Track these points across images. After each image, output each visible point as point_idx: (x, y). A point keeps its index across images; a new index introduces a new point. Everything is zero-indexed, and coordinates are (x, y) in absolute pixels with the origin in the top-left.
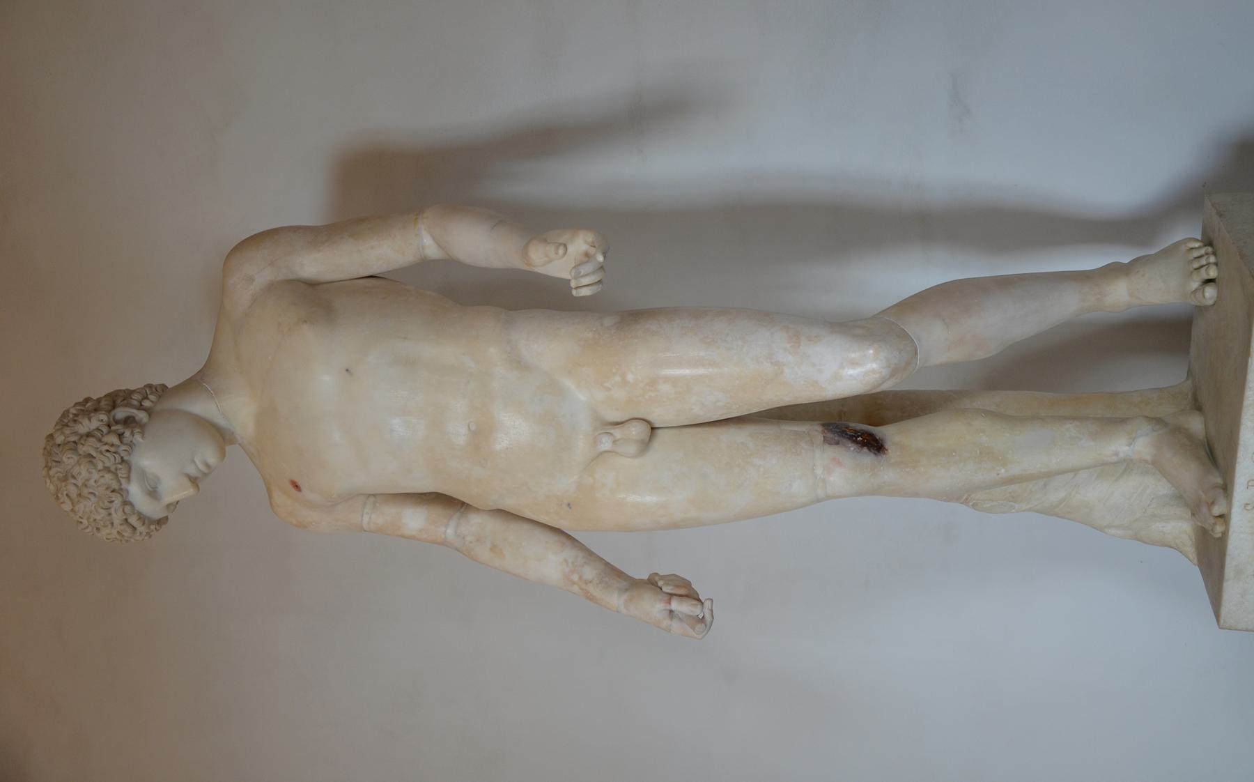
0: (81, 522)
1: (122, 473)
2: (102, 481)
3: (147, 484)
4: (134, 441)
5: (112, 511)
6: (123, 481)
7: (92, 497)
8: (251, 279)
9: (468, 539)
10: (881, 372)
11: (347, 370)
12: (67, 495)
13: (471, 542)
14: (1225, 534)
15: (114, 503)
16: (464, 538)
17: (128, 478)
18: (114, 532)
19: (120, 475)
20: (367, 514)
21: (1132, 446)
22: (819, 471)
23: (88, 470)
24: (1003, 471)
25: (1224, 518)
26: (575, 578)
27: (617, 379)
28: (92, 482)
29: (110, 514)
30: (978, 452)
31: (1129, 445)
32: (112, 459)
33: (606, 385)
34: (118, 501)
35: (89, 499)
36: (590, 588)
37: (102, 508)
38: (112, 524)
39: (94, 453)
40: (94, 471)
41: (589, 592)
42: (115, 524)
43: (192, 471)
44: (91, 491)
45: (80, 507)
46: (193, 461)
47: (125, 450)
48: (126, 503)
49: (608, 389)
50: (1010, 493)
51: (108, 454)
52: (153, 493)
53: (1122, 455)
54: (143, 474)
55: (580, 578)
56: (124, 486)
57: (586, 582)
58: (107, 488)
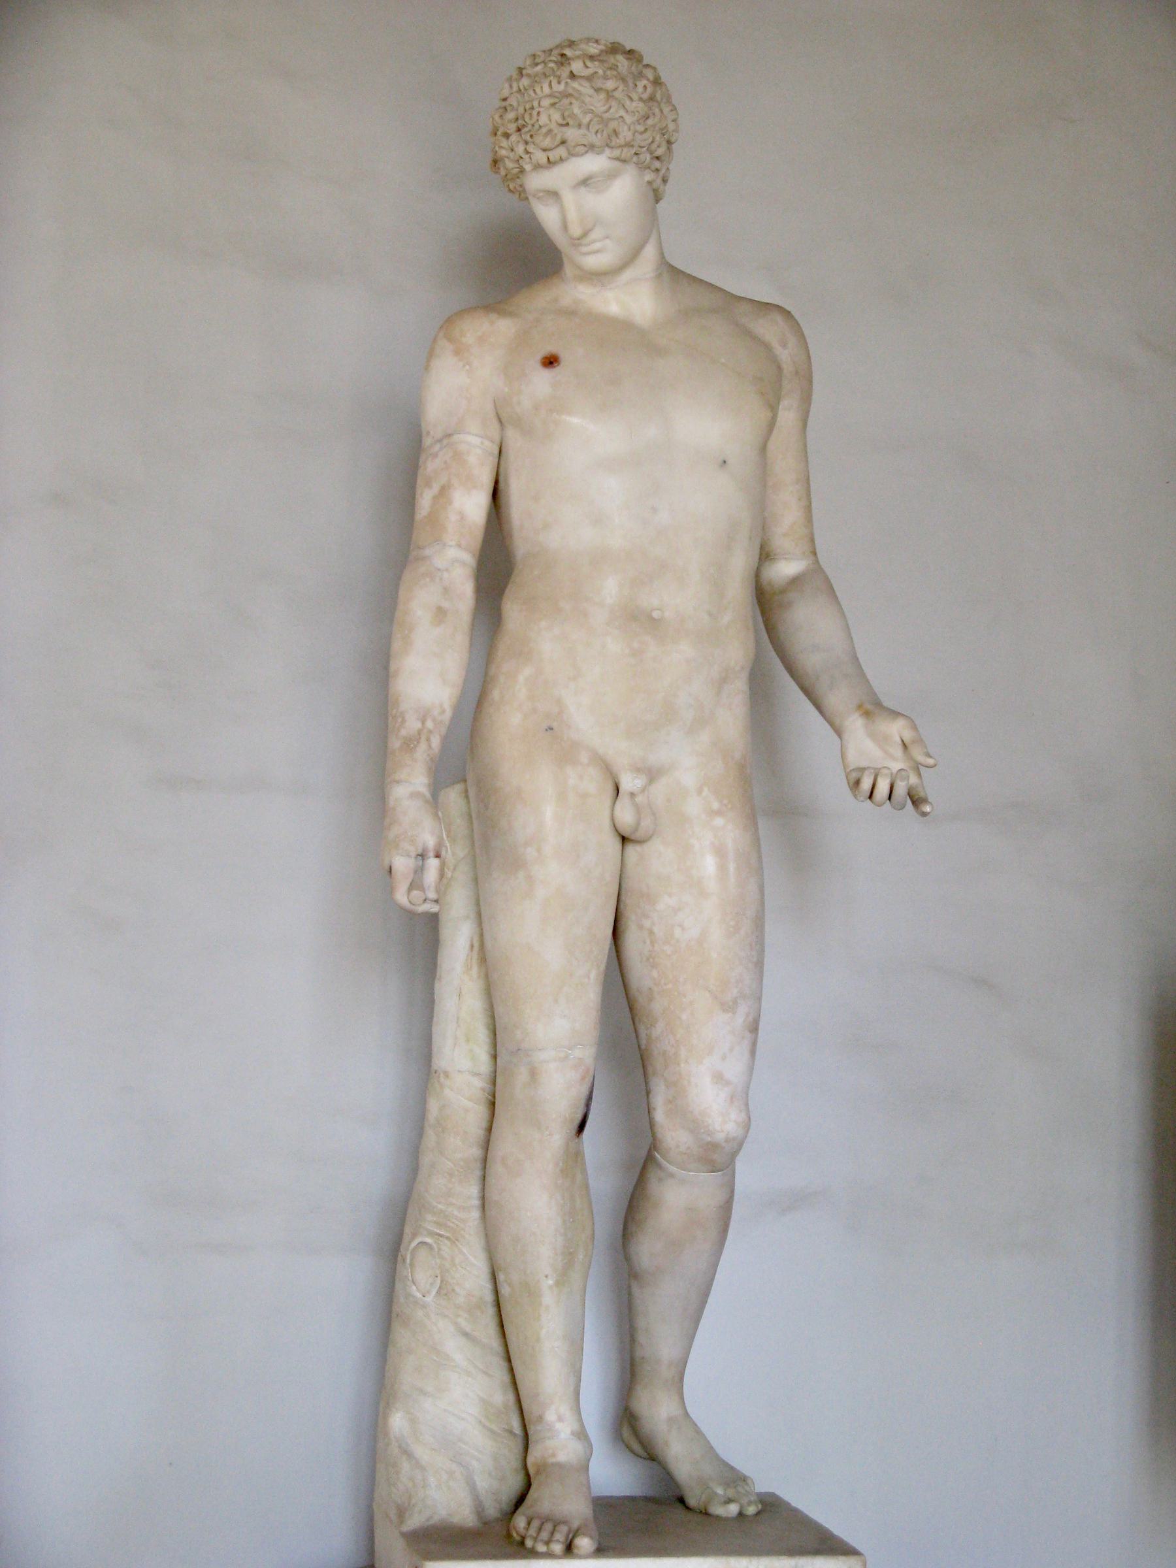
0: (559, 83)
1: (627, 153)
2: (626, 128)
3: (600, 179)
4: (647, 171)
5: (583, 131)
6: (617, 153)
7: (605, 108)
8: (784, 345)
9: (446, 575)
10: (723, 1131)
11: (725, 462)
12: (596, 73)
13: (441, 579)
14: (549, 1555)
15: (594, 136)
16: (447, 570)
17: (618, 159)
18: (553, 126)
19: (625, 150)
20: (482, 443)
21: (572, 1437)
22: (578, 1053)
23: (638, 112)
24: (551, 1282)
25: (569, 1549)
26: (429, 724)
27: (716, 805)
28: (622, 113)
29: (580, 126)
30: (571, 1250)
31: (573, 1433)
32: (643, 144)
33: (706, 791)
34: (597, 140)
35: (604, 106)
36: (423, 746)
37: (591, 121)
38: (567, 124)
39: (650, 122)
40: (635, 118)
41: (418, 742)
42: (564, 129)
43: (595, 234)
44: (612, 110)
45: (584, 88)
46: (607, 237)
47: (646, 159)
48: (591, 148)
49: (700, 791)
50: (453, 1290)
51: (650, 140)
52: (585, 182)
53: (558, 1426)
54: (611, 176)
55: (430, 732)
56: (608, 151)
57: (428, 740)
58: (615, 131)
